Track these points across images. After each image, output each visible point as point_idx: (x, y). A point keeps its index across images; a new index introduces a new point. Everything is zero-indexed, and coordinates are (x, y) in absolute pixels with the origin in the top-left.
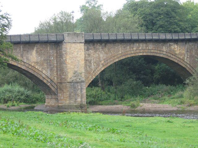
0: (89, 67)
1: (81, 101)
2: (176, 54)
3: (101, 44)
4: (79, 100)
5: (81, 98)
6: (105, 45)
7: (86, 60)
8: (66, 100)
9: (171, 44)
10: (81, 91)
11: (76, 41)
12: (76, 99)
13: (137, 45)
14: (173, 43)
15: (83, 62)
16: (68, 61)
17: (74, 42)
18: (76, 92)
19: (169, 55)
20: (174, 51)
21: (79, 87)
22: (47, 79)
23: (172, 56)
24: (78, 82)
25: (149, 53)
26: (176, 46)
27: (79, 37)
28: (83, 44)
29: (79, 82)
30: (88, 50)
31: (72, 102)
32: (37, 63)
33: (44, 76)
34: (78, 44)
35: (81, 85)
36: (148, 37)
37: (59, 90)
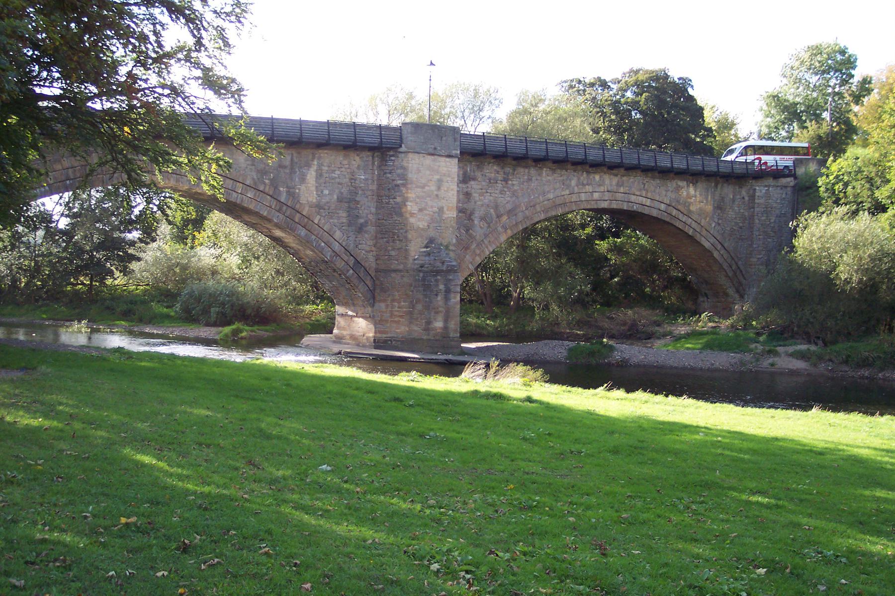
0: (467, 231)
1: (446, 328)
2: (690, 211)
3: (503, 168)
4: (439, 324)
5: (446, 321)
6: (514, 170)
7: (461, 211)
8: (398, 322)
9: (681, 183)
10: (447, 299)
11: (435, 149)
12: (429, 323)
13: (597, 177)
14: (685, 183)
15: (453, 214)
16: (409, 208)
17: (431, 151)
18: (431, 302)
19: (674, 212)
20: (687, 205)
21: (442, 287)
22: (346, 258)
23: (681, 216)
24: (438, 272)
25: (625, 204)
26: (692, 190)
27: (444, 138)
28: (457, 160)
29: (442, 271)
30: (465, 179)
31: (416, 328)
32: (319, 207)
33: (336, 247)
34: (443, 159)
35: (447, 283)
36: (646, 159)
37: (378, 291)
